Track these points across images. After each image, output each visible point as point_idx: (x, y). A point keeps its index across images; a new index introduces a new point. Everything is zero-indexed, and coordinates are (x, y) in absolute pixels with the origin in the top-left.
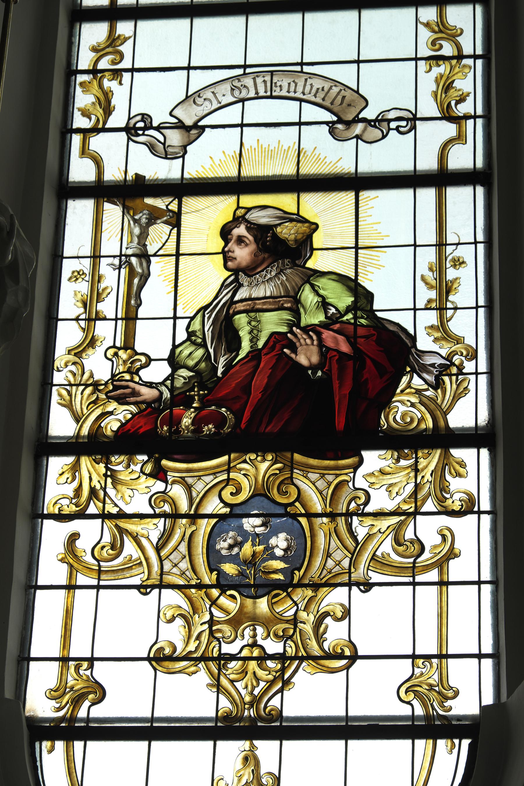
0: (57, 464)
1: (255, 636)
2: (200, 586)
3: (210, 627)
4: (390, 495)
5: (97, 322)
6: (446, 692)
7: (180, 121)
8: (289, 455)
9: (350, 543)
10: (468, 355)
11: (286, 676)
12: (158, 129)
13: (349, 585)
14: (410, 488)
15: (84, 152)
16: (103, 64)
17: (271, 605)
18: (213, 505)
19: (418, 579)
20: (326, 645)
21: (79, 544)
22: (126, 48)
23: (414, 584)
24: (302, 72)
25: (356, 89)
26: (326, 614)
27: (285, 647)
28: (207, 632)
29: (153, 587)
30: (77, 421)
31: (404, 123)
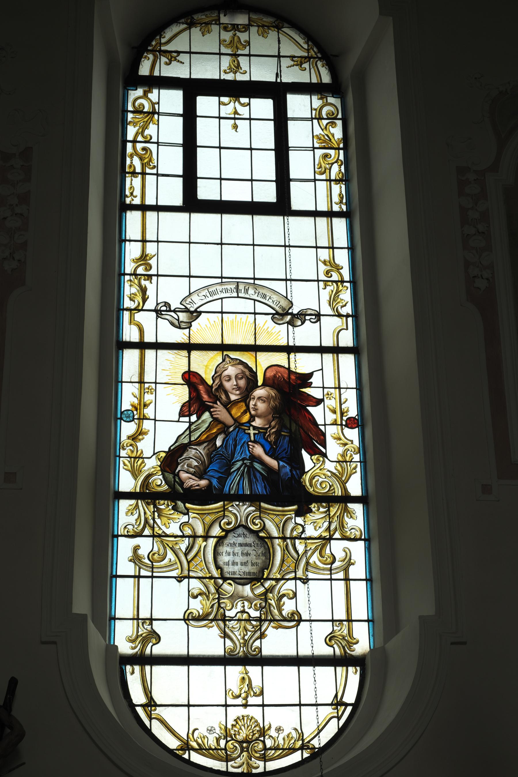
0: (124, 505)
1: (244, 607)
2: (211, 578)
3: (218, 601)
4: (315, 529)
5: (144, 421)
6: (350, 641)
7: (186, 308)
8: (258, 503)
9: (295, 555)
10: (355, 451)
11: (263, 629)
12: (174, 311)
13: (295, 578)
14: (326, 524)
15: (131, 321)
16: (141, 270)
17: (252, 590)
18: (216, 531)
19: (334, 577)
20: (284, 613)
21: (140, 552)
22: (153, 262)
23: (331, 579)
24: (254, 283)
25: (285, 296)
26: (284, 595)
27: (260, 614)
28: (217, 604)
29: (185, 577)
30: (136, 479)
31: (314, 317)
